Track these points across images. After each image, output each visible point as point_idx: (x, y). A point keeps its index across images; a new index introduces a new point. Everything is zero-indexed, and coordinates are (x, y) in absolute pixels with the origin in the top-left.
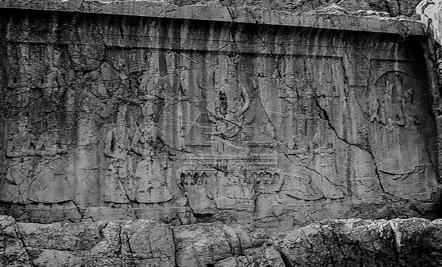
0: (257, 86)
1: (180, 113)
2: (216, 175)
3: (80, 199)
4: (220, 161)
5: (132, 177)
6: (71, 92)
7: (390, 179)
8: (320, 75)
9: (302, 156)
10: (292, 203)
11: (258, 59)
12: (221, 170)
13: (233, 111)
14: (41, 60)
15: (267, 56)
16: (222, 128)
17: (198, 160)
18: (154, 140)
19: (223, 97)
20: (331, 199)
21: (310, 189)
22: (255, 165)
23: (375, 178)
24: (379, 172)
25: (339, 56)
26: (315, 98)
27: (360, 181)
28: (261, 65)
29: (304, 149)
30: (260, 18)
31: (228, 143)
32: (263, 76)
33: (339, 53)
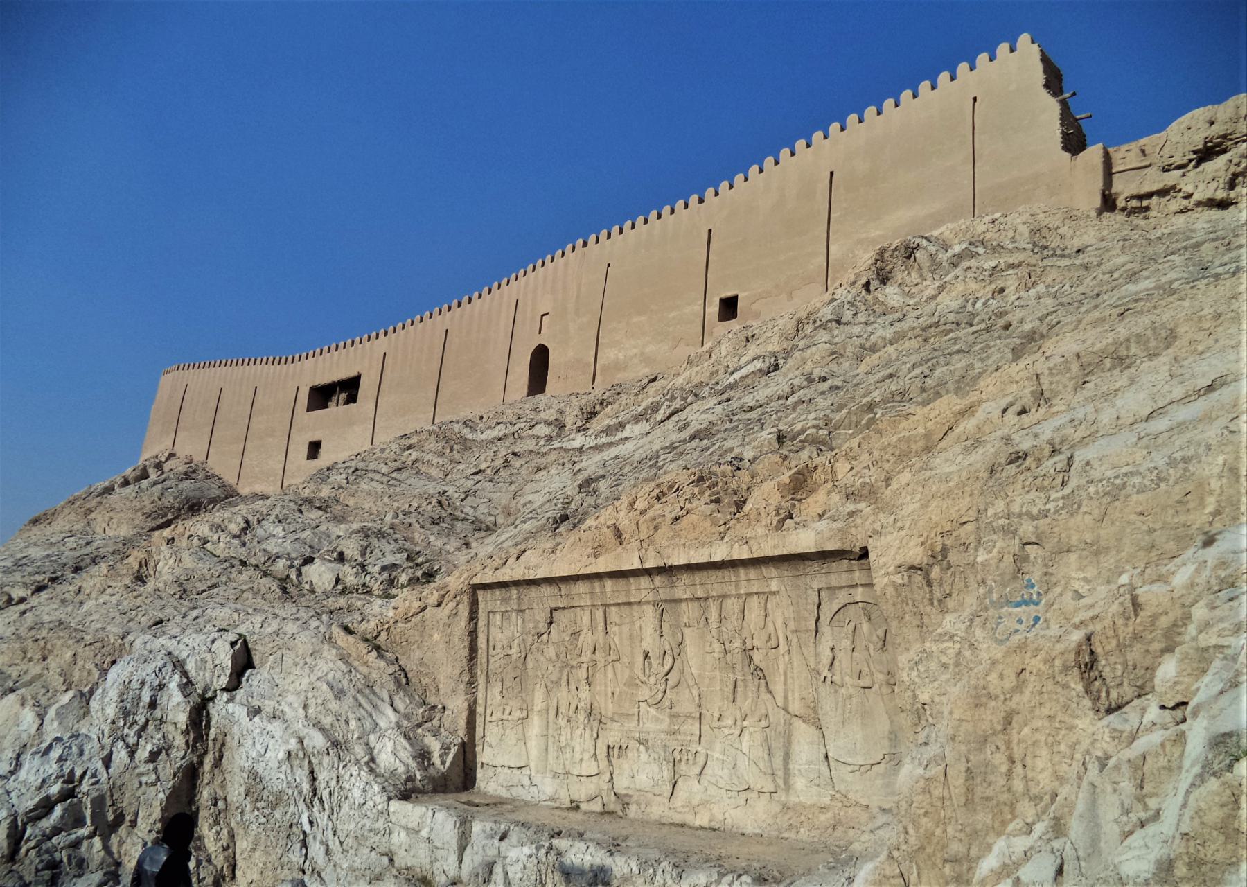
1: (610, 674)
3: (532, 765)
6: (530, 657)
7: (845, 770)
9: (726, 731)
10: (712, 790)
11: (684, 605)
15: (691, 600)
16: (644, 693)
19: (646, 656)
23: (824, 768)
25: (774, 589)
26: (747, 652)
28: (689, 612)
29: (730, 722)
31: (652, 711)
33: (774, 586)
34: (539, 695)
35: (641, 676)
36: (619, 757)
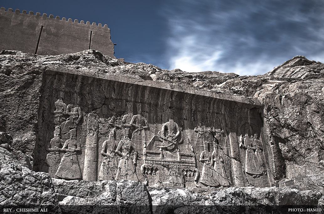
0: (184, 124)
2: (163, 169)
4: (165, 162)
5: (116, 167)
8: (214, 122)
12: (166, 167)
13: (172, 136)
14: (70, 100)
17: (153, 161)
18: (129, 148)
20: (223, 186)
21: (212, 180)
22: (184, 165)
24: (246, 173)
27: (237, 177)
29: (208, 159)
30: (185, 90)
32: (186, 120)
34: (90, 141)
35: (163, 137)
36: (151, 174)
